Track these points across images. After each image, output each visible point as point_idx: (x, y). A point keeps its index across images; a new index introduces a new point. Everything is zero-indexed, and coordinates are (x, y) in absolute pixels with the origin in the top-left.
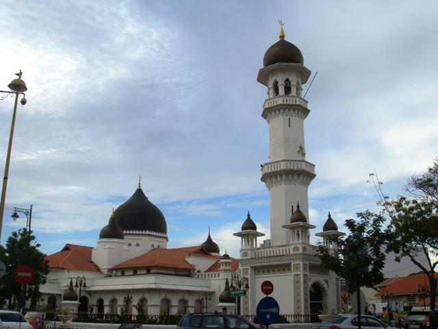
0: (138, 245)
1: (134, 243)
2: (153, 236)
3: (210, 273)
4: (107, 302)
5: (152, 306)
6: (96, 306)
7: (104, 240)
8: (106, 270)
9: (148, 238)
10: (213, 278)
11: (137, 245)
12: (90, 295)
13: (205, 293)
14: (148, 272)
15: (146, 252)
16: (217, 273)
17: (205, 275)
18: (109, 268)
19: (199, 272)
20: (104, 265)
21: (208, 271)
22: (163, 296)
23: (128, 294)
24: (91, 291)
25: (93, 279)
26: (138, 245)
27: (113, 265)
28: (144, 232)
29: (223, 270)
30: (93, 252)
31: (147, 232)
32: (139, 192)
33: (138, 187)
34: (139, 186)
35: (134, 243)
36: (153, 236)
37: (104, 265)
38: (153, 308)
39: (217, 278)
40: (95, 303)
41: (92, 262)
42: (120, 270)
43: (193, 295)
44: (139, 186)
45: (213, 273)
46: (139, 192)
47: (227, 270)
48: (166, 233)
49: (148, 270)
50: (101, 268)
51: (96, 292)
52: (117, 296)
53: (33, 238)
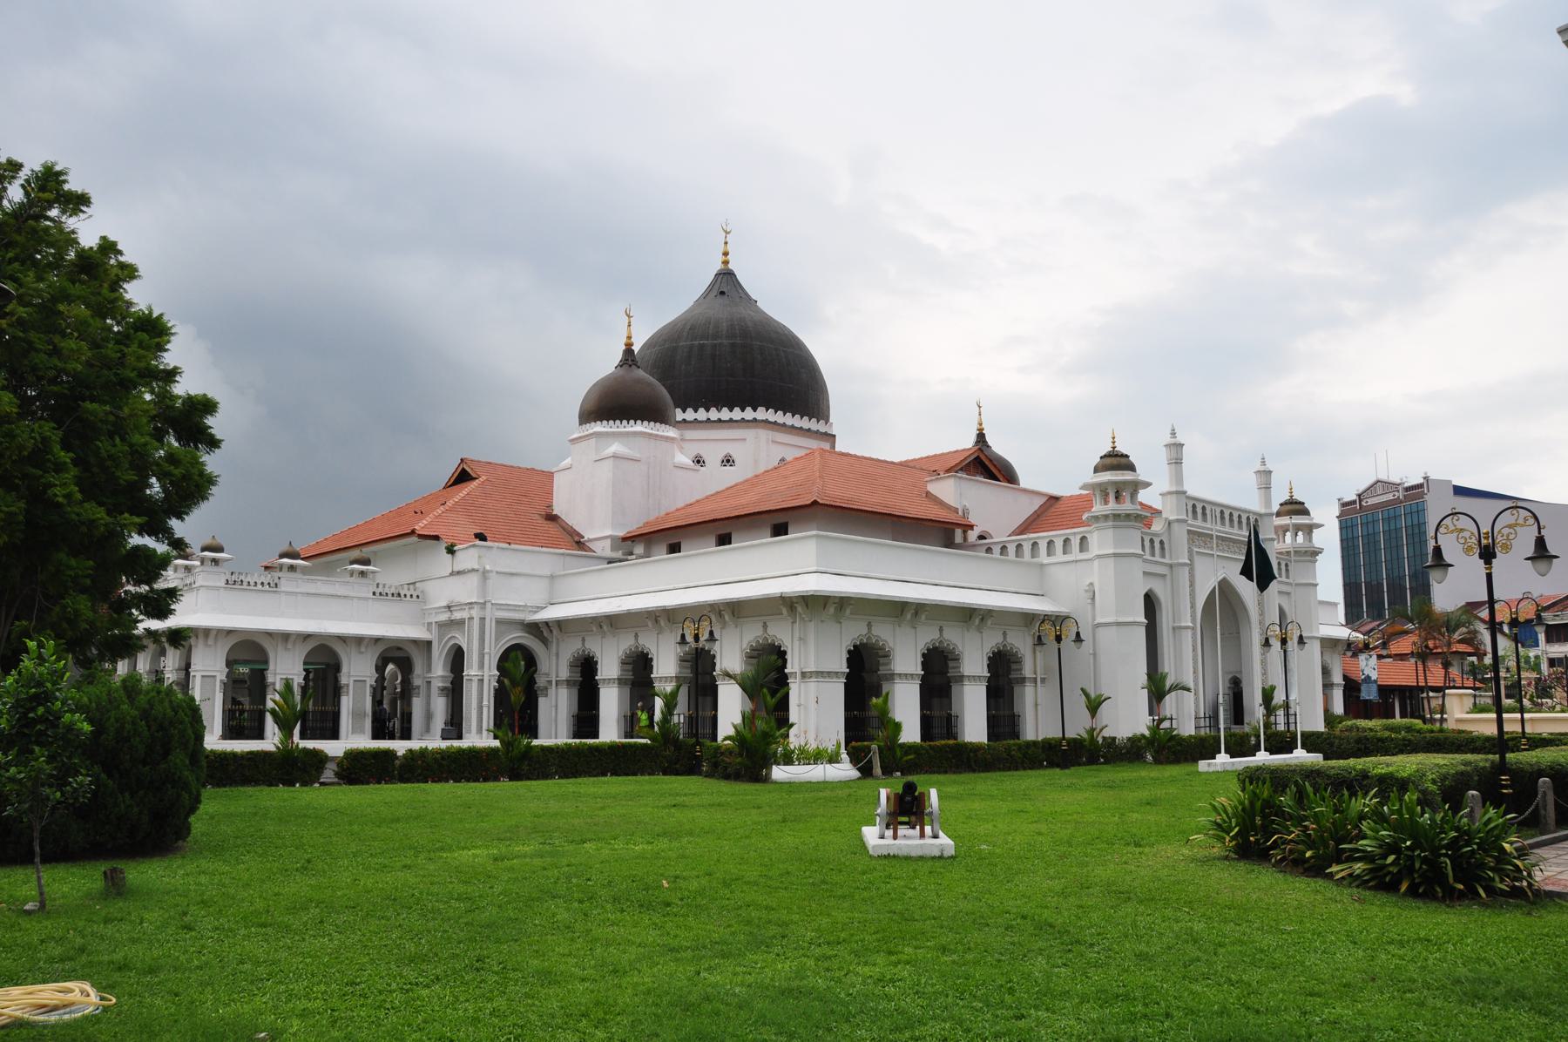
0: (728, 461)
1: (713, 455)
2: (782, 427)
3: (1042, 537)
4: (609, 668)
5: (804, 674)
6: (569, 683)
7: (598, 427)
8: (608, 542)
9: (763, 434)
10: (1059, 556)
11: (737, 453)
12: (545, 641)
13: (1028, 618)
14: (780, 530)
15: (761, 469)
16: (1075, 534)
17: (1019, 546)
18: (622, 533)
19: (981, 537)
20: (599, 528)
21: (1024, 528)
22: (853, 632)
23: (697, 626)
24: (547, 623)
25: (552, 577)
26: (728, 461)
27: (632, 525)
28: (749, 414)
29: (1106, 517)
30: (560, 483)
31: (762, 414)
32: (726, 282)
33: (718, 266)
34: (726, 263)
35: (713, 455)
36: (782, 427)
37: (599, 528)
38: (812, 686)
39: (1075, 554)
40: (564, 673)
41: (552, 518)
42: (668, 537)
43: (979, 630)
44: (726, 263)
45: (1058, 536)
46: (726, 282)
47: (1128, 516)
48: (827, 421)
49: (779, 523)
50: (588, 535)
51: (561, 624)
52: (649, 643)
53: (130, 272)
